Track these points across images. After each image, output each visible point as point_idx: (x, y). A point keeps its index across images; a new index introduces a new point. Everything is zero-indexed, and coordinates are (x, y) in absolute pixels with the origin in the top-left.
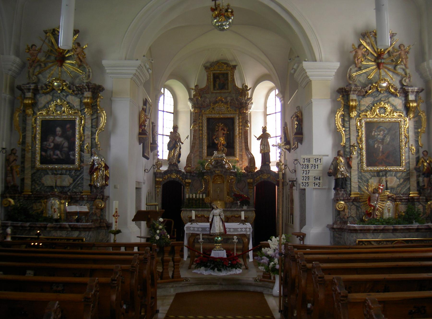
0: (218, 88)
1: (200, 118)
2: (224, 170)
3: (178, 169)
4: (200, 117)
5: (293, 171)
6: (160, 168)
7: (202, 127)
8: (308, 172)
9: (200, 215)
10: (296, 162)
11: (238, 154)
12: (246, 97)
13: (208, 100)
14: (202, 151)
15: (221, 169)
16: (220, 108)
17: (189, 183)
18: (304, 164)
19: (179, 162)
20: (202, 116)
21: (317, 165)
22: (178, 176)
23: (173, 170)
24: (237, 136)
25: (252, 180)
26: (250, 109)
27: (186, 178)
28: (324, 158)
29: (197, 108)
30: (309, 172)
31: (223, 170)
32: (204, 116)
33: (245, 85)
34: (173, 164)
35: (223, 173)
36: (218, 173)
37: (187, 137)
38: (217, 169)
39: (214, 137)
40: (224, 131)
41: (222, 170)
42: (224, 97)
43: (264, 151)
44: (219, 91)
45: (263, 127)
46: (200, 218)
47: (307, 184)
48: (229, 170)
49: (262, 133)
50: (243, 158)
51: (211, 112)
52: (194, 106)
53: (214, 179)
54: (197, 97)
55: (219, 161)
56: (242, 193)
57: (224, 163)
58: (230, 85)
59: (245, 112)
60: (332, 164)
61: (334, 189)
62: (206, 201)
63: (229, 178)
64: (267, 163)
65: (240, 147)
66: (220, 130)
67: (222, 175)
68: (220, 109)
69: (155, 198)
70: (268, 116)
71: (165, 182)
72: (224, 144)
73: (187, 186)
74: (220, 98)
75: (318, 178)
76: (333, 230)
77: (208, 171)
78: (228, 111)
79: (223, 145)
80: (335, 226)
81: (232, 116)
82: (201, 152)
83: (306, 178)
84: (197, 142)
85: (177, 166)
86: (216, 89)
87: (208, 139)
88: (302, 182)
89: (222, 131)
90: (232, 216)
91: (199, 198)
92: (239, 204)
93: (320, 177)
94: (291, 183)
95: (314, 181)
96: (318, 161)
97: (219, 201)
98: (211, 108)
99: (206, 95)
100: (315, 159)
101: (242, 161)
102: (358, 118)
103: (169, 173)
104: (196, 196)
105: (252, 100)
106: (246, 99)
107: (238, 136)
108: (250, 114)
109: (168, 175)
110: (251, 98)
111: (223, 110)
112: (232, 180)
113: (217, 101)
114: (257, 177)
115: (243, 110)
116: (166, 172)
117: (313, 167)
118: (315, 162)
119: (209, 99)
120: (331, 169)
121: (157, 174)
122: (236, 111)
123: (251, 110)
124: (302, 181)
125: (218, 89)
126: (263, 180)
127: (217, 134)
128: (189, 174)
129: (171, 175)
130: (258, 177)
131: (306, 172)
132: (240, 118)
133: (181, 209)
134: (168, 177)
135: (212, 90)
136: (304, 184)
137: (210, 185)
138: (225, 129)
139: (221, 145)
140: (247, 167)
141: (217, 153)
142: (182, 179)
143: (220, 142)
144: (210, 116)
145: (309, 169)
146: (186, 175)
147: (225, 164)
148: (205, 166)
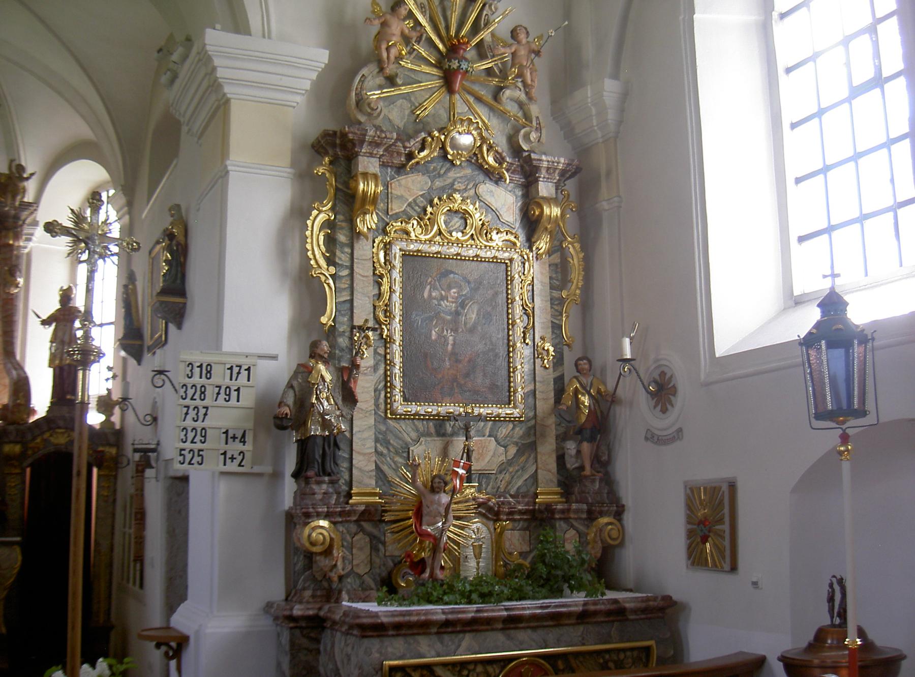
5: (149, 418)
8: (202, 411)
10: (158, 381)
12: (19, 198)
18: (190, 382)
21: (238, 390)
25: (17, 448)
26: (29, 240)
28: (262, 363)
30: (205, 414)
43: (61, 360)
45: (62, 287)
47: (199, 455)
49: (58, 306)
60: (290, 386)
61: (296, 475)
75: (239, 435)
76: (292, 625)
80: (298, 611)
83: (193, 434)
88: (181, 450)
93: (245, 431)
94: (141, 457)
95: (223, 447)
96: (239, 373)
100: (231, 368)
102: (380, 238)
106: (17, 204)
108: (29, 255)
114: (34, 438)
115: (6, 237)
117: (222, 396)
118: (231, 379)
120: (288, 406)
123: (31, 245)
124: (182, 445)
126: (51, 449)
130: (38, 440)
131: (197, 414)
136: (188, 457)
145: (205, 403)
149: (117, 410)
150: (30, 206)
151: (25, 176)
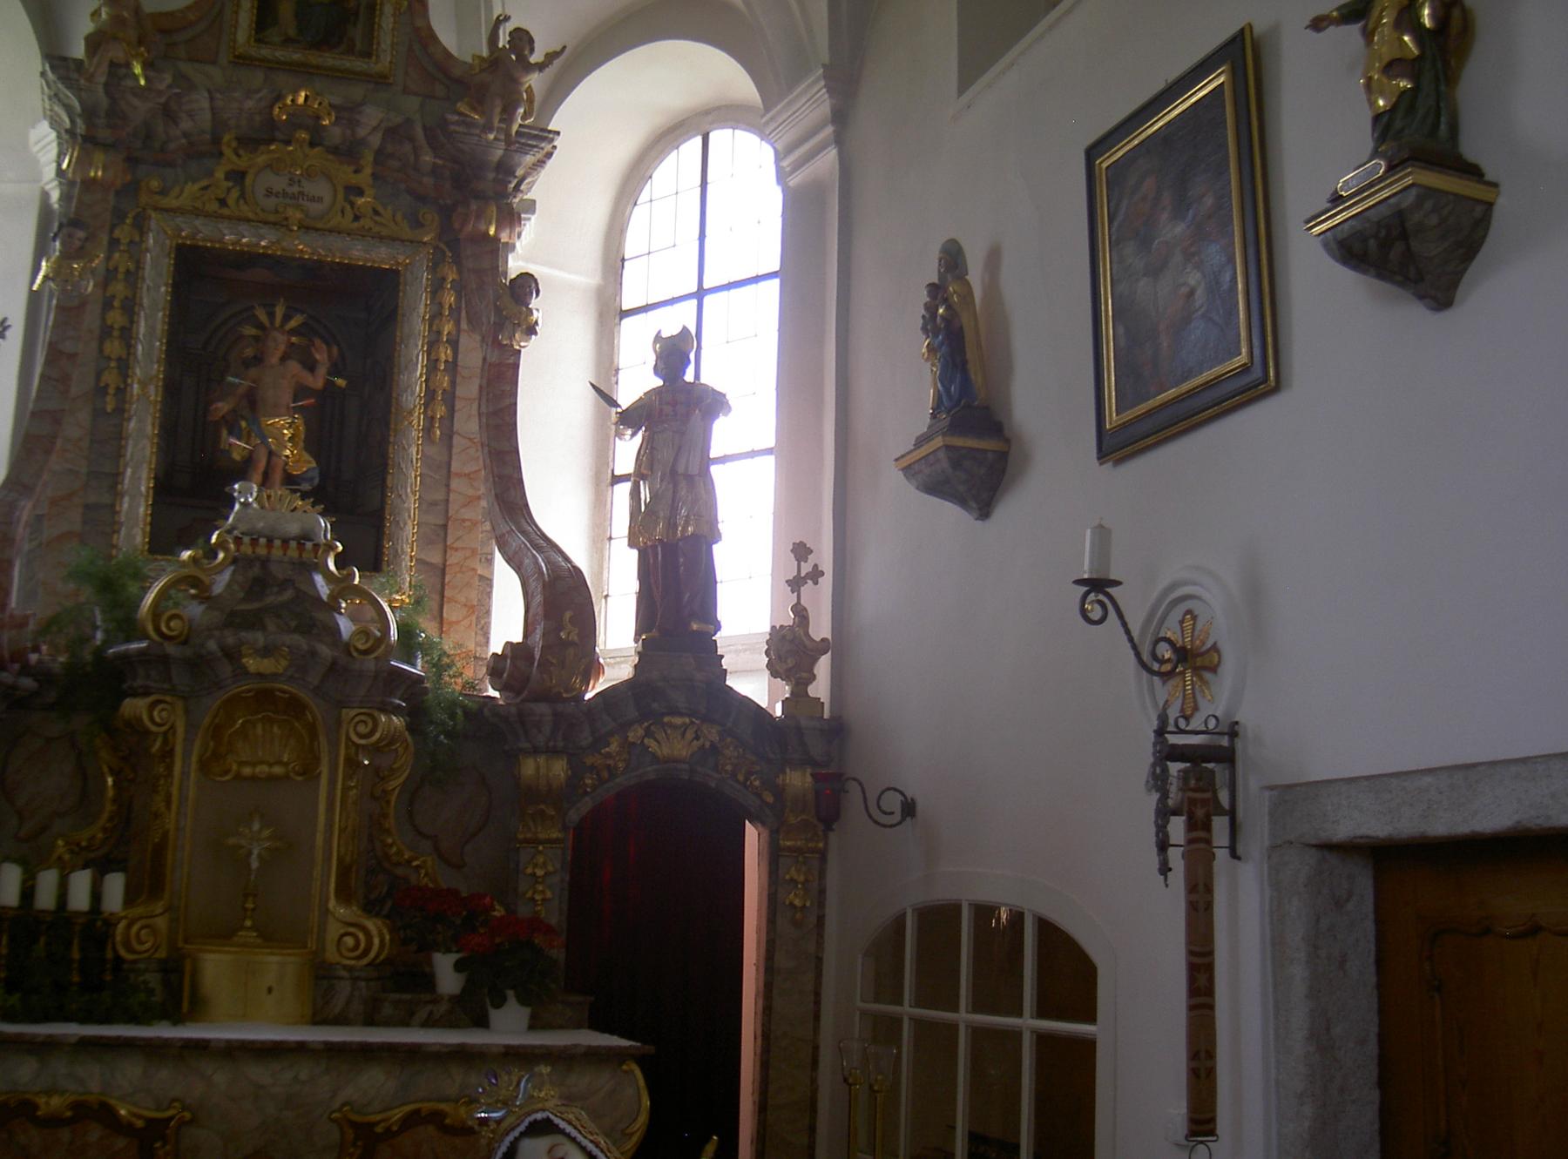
0: (292, 32)
1: (117, 233)
4: (124, 233)
7: (130, 308)
9: (55, 1103)
11: (406, 562)
14: (112, 509)
16: (292, 182)
20: (140, 225)
24: (411, 413)
25: (559, 769)
29: (106, 147)
31: (313, 653)
32: (153, 224)
33: (510, 26)
38: (259, 638)
40: (311, 367)
44: (297, 56)
46: (65, 1134)
48: (366, 652)
50: (447, 593)
51: (214, 206)
53: (216, 731)
54: (117, 52)
55: (278, 571)
57: (323, 587)
59: (496, 239)
62: (131, 950)
63: (362, 729)
64: (695, 626)
65: (434, 504)
66: (274, 360)
67: (304, 696)
68: (295, 189)
70: (626, 322)
77: (170, 649)
78: (357, 218)
79: (290, 480)
81: (381, 256)
82: (102, 519)
89: (294, 366)
90: (412, 1120)
98: (220, 174)
99: (186, 68)
105: (549, 155)
106: (515, 128)
107: (418, 420)
111: (313, 199)
113: (271, 124)
115: (479, 215)
119: (212, 99)
122: (417, 224)
125: (288, 41)
130: (614, 747)
132: (444, 279)
135: (242, 36)
139: (277, 476)
144: (205, 232)
147: (335, 598)
149: (823, 666)
150: (544, 139)
151: (533, 59)
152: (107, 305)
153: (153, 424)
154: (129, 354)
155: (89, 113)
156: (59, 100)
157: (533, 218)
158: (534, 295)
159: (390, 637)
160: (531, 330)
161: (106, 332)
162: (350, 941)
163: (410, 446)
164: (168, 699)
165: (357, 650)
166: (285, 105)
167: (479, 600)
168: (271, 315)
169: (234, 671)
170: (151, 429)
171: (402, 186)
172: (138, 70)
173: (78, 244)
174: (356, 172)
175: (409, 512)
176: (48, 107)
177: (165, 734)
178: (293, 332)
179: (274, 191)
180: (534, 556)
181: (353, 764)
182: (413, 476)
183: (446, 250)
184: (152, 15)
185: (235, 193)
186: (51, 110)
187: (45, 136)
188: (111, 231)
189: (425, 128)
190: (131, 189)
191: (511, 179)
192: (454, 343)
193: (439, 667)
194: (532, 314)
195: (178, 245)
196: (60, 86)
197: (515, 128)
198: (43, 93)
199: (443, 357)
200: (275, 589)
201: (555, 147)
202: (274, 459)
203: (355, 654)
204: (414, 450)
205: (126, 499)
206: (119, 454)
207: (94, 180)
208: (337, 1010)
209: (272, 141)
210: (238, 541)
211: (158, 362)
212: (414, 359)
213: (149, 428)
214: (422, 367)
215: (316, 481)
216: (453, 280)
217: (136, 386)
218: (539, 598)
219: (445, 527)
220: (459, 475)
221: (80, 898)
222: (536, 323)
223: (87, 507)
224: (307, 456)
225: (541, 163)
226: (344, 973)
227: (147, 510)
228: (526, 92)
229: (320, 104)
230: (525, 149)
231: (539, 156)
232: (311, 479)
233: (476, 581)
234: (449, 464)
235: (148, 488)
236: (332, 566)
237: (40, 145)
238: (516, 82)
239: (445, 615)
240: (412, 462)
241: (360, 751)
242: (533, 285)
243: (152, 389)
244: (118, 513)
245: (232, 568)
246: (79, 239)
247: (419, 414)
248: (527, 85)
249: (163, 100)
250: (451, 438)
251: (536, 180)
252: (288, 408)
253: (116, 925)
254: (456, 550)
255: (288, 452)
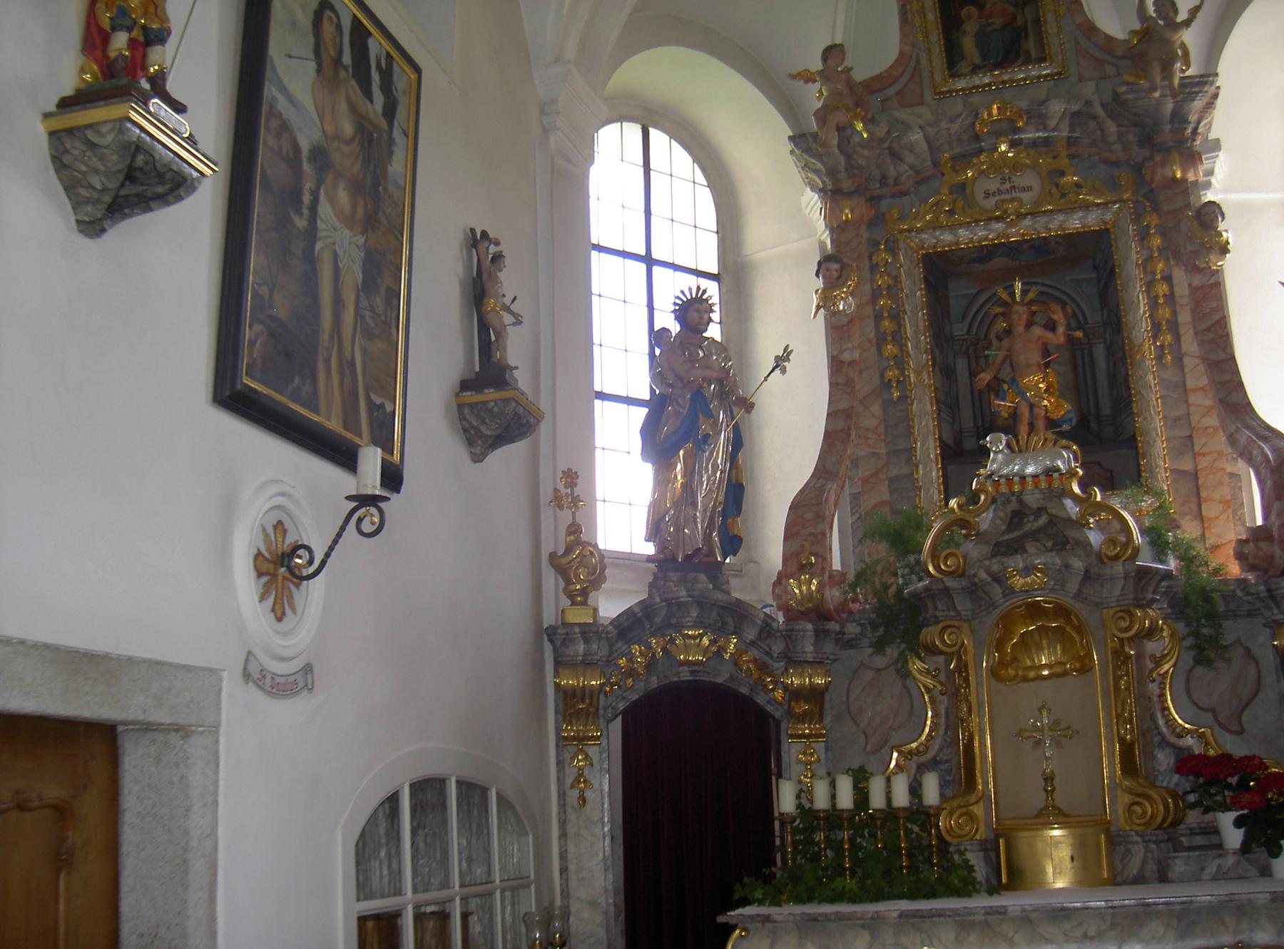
0: (977, 60)
1: (875, 260)
2: (1078, 564)
3: (718, 596)
6: (584, 593)
7: (896, 317)
11: (1162, 475)
13: (916, 136)
15: (1055, 560)
16: (1003, 181)
17: (816, 695)
19: (733, 543)
20: (892, 249)
22: (721, 650)
23: (680, 605)
24: (1141, 345)
26: (1208, 185)
27: (792, 661)
29: (849, 195)
31: (1067, 566)
32: (901, 245)
34: (688, 558)
35: (1073, 586)
36: (1027, 591)
37: (781, 362)
38: (1018, 561)
39: (985, 377)
40: (1051, 326)
41: (1058, 561)
42: (1024, 105)
48: (1116, 558)
50: (1204, 494)
52: (833, 195)
54: (839, 117)
55: (1032, 499)
56: (1238, 749)
57: (1072, 509)
58: (1051, 27)
59: (1184, 180)
63: (1123, 624)
65: (1177, 419)
67: (1068, 601)
68: (1008, 185)
69: (563, 822)
71: (635, 697)
72: (1055, 416)
73: (801, 718)
74: (995, 112)
77: (950, 582)
79: (1051, 424)
82: (905, 485)
84: (872, 417)
85: (715, 571)
86: (963, 67)
87: (947, 405)
89: (1037, 331)
91: (890, 813)
92: (1234, 837)
97: (1062, 825)
99: (901, 114)
101: (1200, 517)
103: (653, 635)
104: (862, 796)
105: (1216, 96)
106: (1176, 81)
107: (1148, 352)
109: (649, 647)
110: (1207, 78)
111: (1023, 190)
112: (1151, 647)
115: (1164, 164)
116: (628, 626)
121: (568, 640)
125: (976, 69)
127: (1002, 354)
128: (810, 626)
129: (672, 641)
132: (1148, 227)
133: (721, 919)
134: (651, 665)
135: (938, 77)
137: (973, 699)
138: (1058, 316)
139: (1041, 424)
140: (1259, 535)
141: (1008, 445)
142: (764, 668)
143: (1032, 406)
146: (789, 636)
147: (1084, 515)
148: (919, 550)
150: (1205, 83)
152: (878, 318)
153: (931, 404)
154: (902, 351)
155: (832, 173)
156: (809, 168)
157: (1221, 154)
158: (1220, 219)
159: (1134, 541)
160: (1224, 249)
161: (881, 341)
162: (1138, 809)
163: (1147, 374)
164: (956, 624)
165: (1108, 557)
166: (983, 120)
167: (1233, 495)
168: (1012, 294)
169: (1003, 592)
170: (930, 408)
171: (1097, 158)
172: (860, 126)
173: (836, 274)
174: (1055, 157)
175: (1157, 430)
176: (804, 176)
177: (958, 652)
178: (1031, 303)
179: (990, 192)
180: (1260, 446)
181: (1119, 654)
182: (1154, 399)
183: (1145, 201)
184: (860, 83)
185: (960, 203)
186: (807, 178)
187: (812, 198)
188: (870, 259)
189: (1103, 105)
190: (877, 221)
191: (1185, 126)
192: (1168, 279)
193: (1188, 560)
194: (1222, 236)
195: (924, 256)
196: (805, 156)
197: (1176, 81)
198: (797, 166)
199: (1161, 293)
200: (1032, 518)
201: (1219, 88)
202: (1036, 410)
203: (1106, 560)
204: (1151, 377)
205: (921, 466)
206: (909, 433)
207: (847, 220)
208: (1135, 872)
209: (981, 151)
210: (996, 484)
211: (926, 352)
212: (1136, 301)
213: (928, 407)
214: (1144, 305)
215: (1075, 421)
216: (1156, 226)
217: (912, 375)
218: (1269, 483)
219: (1190, 437)
220: (1194, 390)
221: (901, 798)
222: (1228, 243)
223: (892, 480)
224: (1062, 401)
225: (1210, 105)
226: (1138, 839)
227: (938, 472)
228: (1180, 48)
229: (1011, 112)
230: (1192, 97)
231: (1206, 100)
232: (1071, 420)
233: (1226, 479)
234: (1184, 382)
235: (936, 454)
236: (1076, 489)
237: (810, 207)
238: (1168, 43)
239: (1204, 513)
240: (1151, 387)
241: (1126, 643)
242: (1217, 210)
243: (925, 375)
244: (917, 479)
245: (993, 507)
246: (836, 271)
247: (1150, 345)
248: (1179, 42)
249: (887, 145)
250: (1181, 359)
251: (1212, 118)
252: (1039, 365)
253: (937, 816)
254: (1204, 455)
255: (1046, 402)
